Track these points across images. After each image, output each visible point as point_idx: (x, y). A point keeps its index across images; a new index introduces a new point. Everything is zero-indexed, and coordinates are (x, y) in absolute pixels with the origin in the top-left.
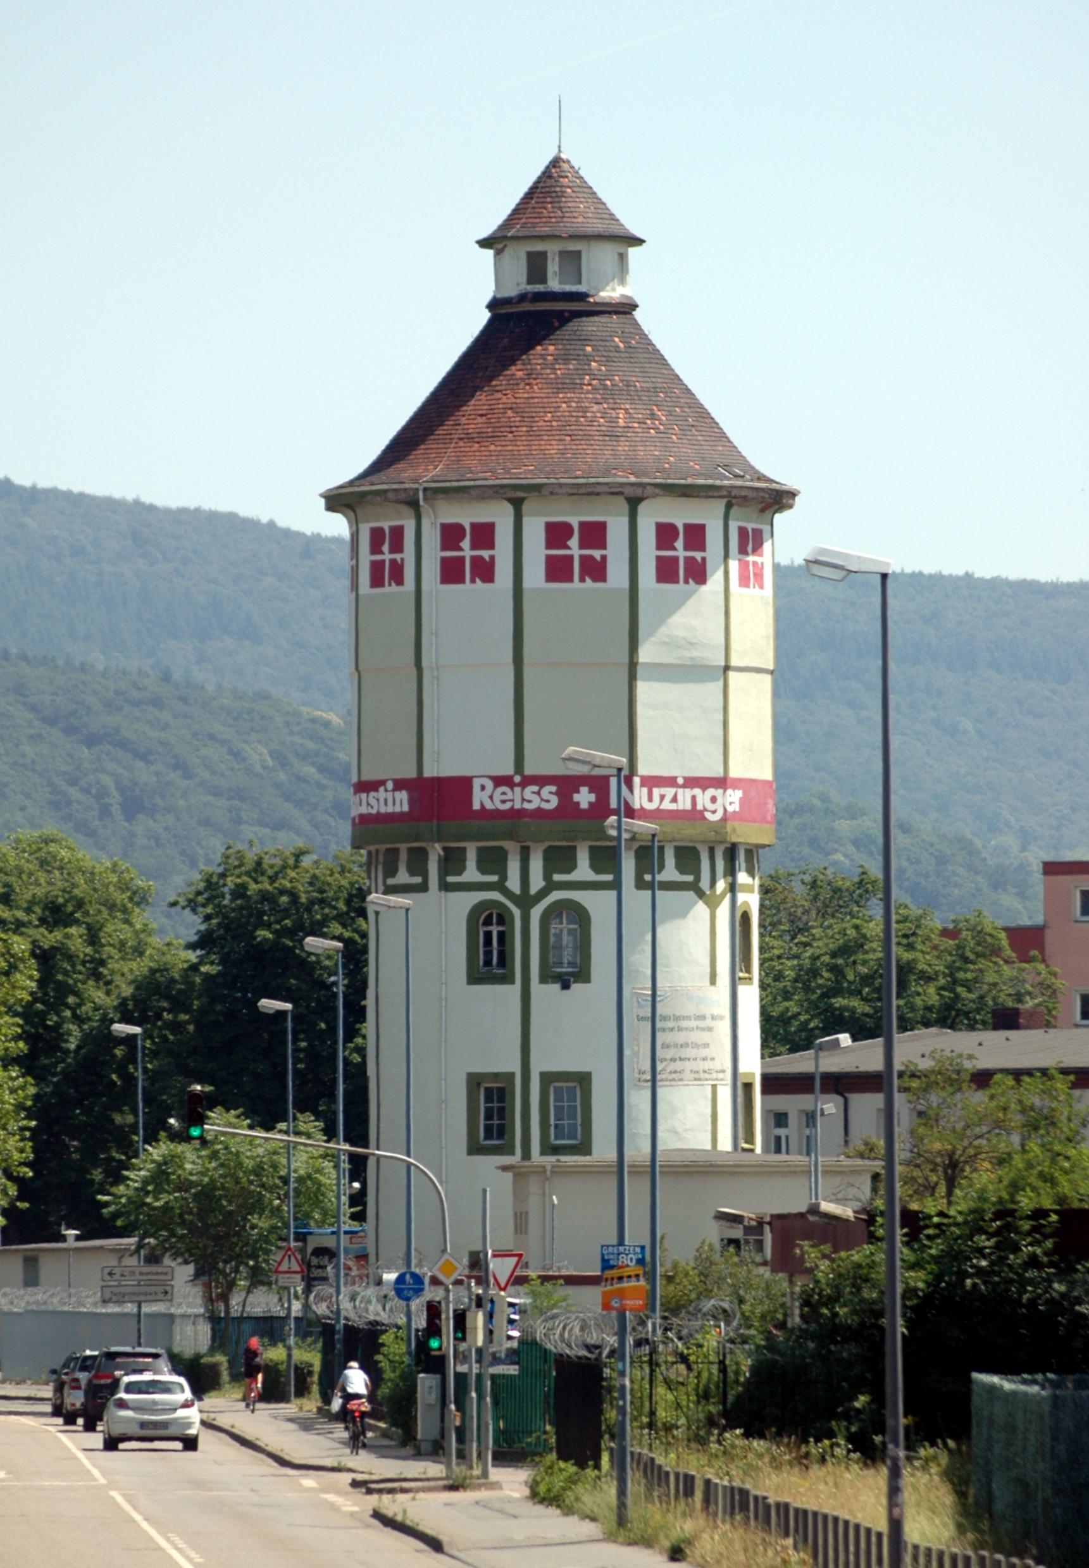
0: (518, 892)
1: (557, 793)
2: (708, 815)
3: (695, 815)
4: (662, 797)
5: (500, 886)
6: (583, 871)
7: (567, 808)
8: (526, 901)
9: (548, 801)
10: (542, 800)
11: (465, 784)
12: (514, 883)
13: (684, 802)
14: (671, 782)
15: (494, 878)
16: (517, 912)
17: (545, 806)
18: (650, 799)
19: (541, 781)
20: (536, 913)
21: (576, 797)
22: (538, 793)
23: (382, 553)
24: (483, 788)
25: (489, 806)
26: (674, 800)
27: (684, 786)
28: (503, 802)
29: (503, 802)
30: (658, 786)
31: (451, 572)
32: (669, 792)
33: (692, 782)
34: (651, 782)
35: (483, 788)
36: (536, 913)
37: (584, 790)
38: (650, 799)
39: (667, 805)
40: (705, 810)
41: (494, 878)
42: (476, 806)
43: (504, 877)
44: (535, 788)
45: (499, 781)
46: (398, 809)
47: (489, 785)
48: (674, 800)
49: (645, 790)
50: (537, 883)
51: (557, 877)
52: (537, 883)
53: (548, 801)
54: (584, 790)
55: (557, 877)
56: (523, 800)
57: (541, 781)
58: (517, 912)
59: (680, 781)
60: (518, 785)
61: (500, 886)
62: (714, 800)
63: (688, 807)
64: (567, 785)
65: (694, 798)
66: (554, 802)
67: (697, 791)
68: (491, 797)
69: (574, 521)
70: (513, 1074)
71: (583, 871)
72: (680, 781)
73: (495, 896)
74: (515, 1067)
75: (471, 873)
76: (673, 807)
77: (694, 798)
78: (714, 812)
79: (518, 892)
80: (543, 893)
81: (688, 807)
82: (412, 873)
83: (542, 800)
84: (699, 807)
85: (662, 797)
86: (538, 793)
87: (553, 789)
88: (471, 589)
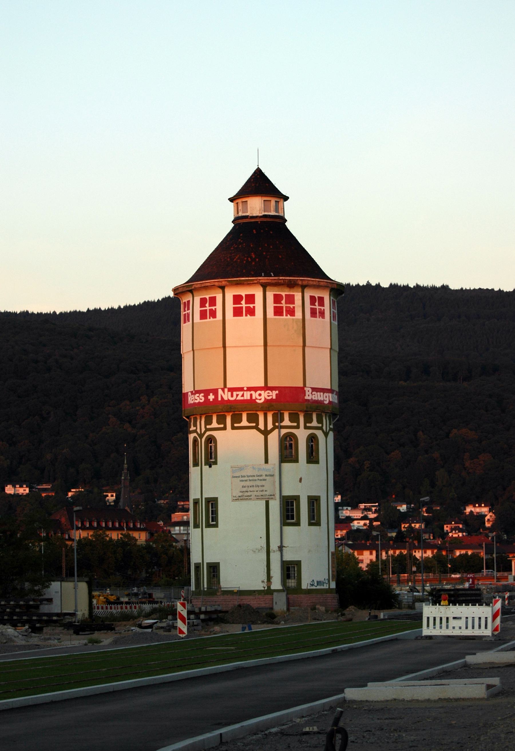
0: (263, 429)
12: (261, 426)
15: (254, 424)
23: (206, 307)
31: (237, 312)
41: (254, 424)
43: (258, 424)
50: (270, 426)
52: (270, 426)
69: (283, 294)
79: (263, 429)
88: (245, 319)
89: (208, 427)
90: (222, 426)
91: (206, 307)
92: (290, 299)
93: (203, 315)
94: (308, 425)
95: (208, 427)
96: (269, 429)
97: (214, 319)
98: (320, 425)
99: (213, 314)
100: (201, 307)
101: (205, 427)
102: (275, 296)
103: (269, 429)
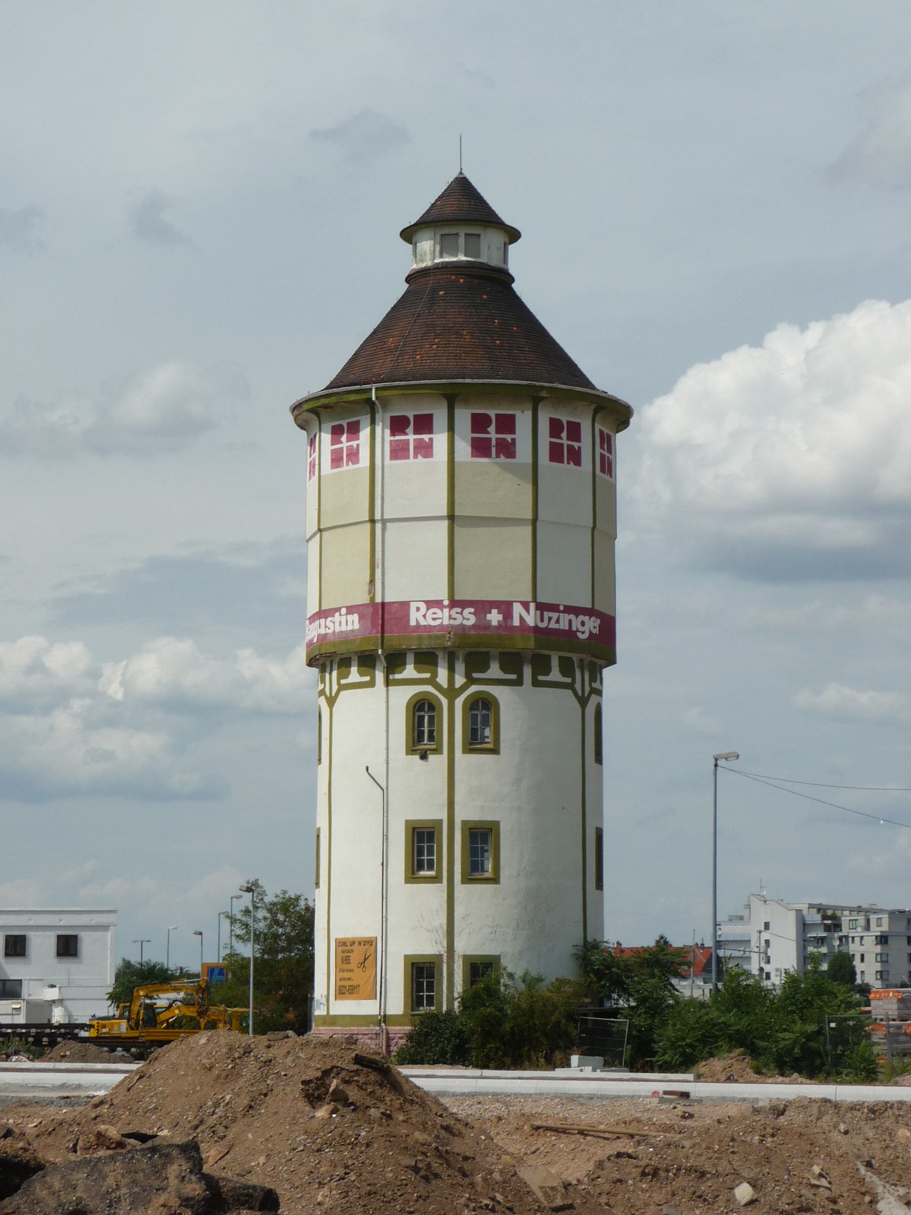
1: (474, 614)
2: (579, 634)
3: (570, 634)
4: (550, 619)
5: (432, 681)
6: (495, 671)
7: (482, 626)
8: (452, 693)
9: (468, 619)
10: (464, 618)
11: (405, 606)
13: (563, 625)
14: (554, 608)
15: (427, 675)
16: (444, 701)
17: (466, 622)
18: (542, 620)
19: (464, 604)
20: (459, 702)
21: (489, 617)
22: (461, 613)
23: (342, 443)
24: (418, 609)
25: (423, 622)
26: (558, 621)
27: (564, 612)
28: (434, 619)
29: (434, 619)
30: (549, 611)
32: (555, 615)
33: (569, 610)
34: (542, 607)
35: (418, 609)
36: (459, 702)
37: (495, 611)
38: (542, 620)
39: (553, 625)
40: (578, 631)
41: (427, 675)
42: (413, 623)
43: (435, 675)
44: (459, 610)
45: (430, 604)
46: (350, 628)
47: (423, 607)
48: (558, 621)
49: (538, 612)
51: (475, 675)
53: (468, 619)
54: (495, 611)
55: (475, 675)
56: (450, 617)
57: (464, 604)
58: (444, 701)
59: (562, 608)
60: (446, 607)
61: (432, 681)
62: (583, 624)
63: (567, 628)
64: (482, 607)
65: (570, 621)
66: (472, 620)
67: (572, 617)
68: (424, 616)
70: (441, 821)
71: (495, 671)
72: (562, 608)
73: (429, 688)
74: (443, 815)
75: (410, 671)
76: (556, 626)
77: (570, 621)
78: (583, 633)
80: (464, 688)
81: (567, 628)
82: (361, 674)
83: (464, 618)
84: (574, 629)
85: (550, 619)
86: (461, 613)
87: (472, 610)
89: (343, 682)
90: (367, 679)
91: (342, 443)
92: (507, 424)
93: (337, 460)
94: (541, 678)
95: (343, 682)
96: (457, 685)
97: (356, 466)
98: (569, 680)
99: (353, 455)
100: (333, 444)
101: (339, 683)
102: (474, 417)
103: (457, 685)
